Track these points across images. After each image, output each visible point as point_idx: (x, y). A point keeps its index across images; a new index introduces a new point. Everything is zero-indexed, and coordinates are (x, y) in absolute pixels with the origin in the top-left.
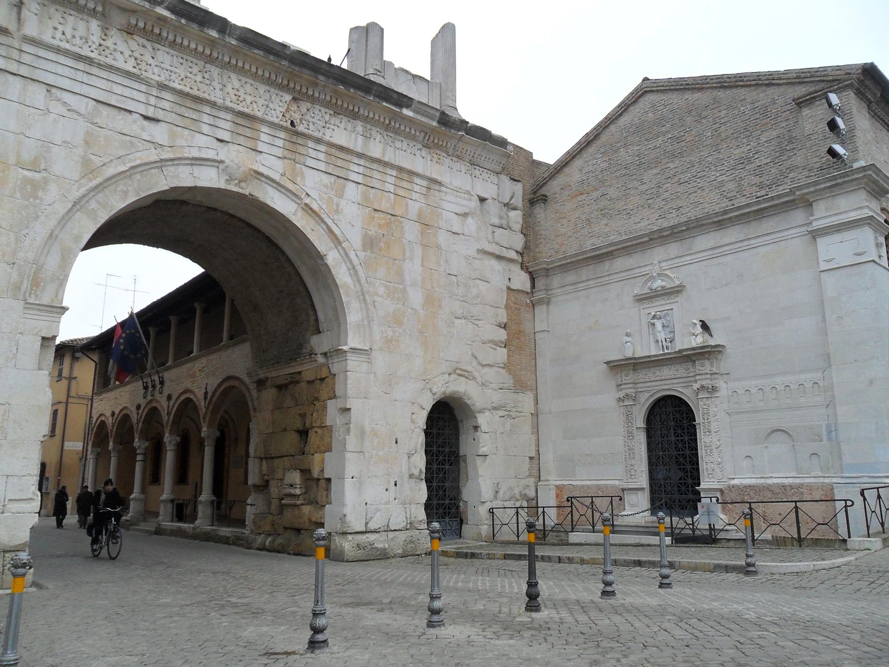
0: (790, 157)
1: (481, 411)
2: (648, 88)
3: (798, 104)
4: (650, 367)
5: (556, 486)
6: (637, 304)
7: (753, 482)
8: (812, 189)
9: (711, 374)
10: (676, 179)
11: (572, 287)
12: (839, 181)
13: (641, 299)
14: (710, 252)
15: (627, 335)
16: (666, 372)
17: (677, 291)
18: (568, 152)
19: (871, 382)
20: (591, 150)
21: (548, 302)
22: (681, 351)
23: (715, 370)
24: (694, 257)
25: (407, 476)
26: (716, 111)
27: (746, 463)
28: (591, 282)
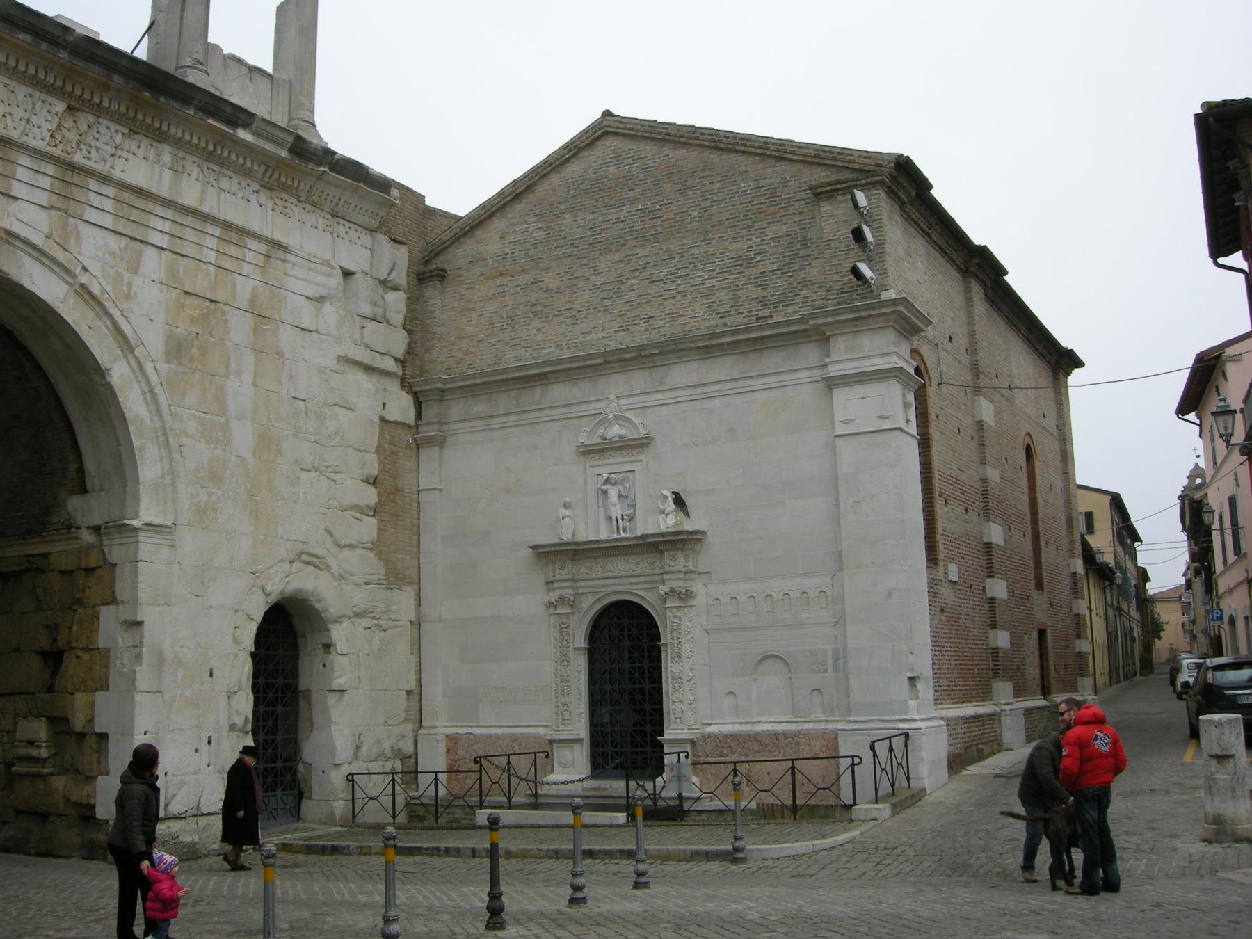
0: (802, 268)
1: (336, 621)
2: (608, 128)
3: (817, 195)
4: (597, 557)
5: (448, 736)
7: (736, 728)
8: (830, 320)
9: (686, 573)
10: (646, 274)
11: (480, 423)
12: (864, 314)
13: (587, 452)
14: (690, 391)
15: (566, 506)
16: (622, 566)
17: (642, 444)
18: (483, 206)
19: (890, 594)
20: (520, 207)
21: (441, 442)
22: (644, 537)
23: (691, 567)
24: (668, 395)
25: (226, 728)
26: (706, 181)
27: (727, 702)
28: (512, 418)
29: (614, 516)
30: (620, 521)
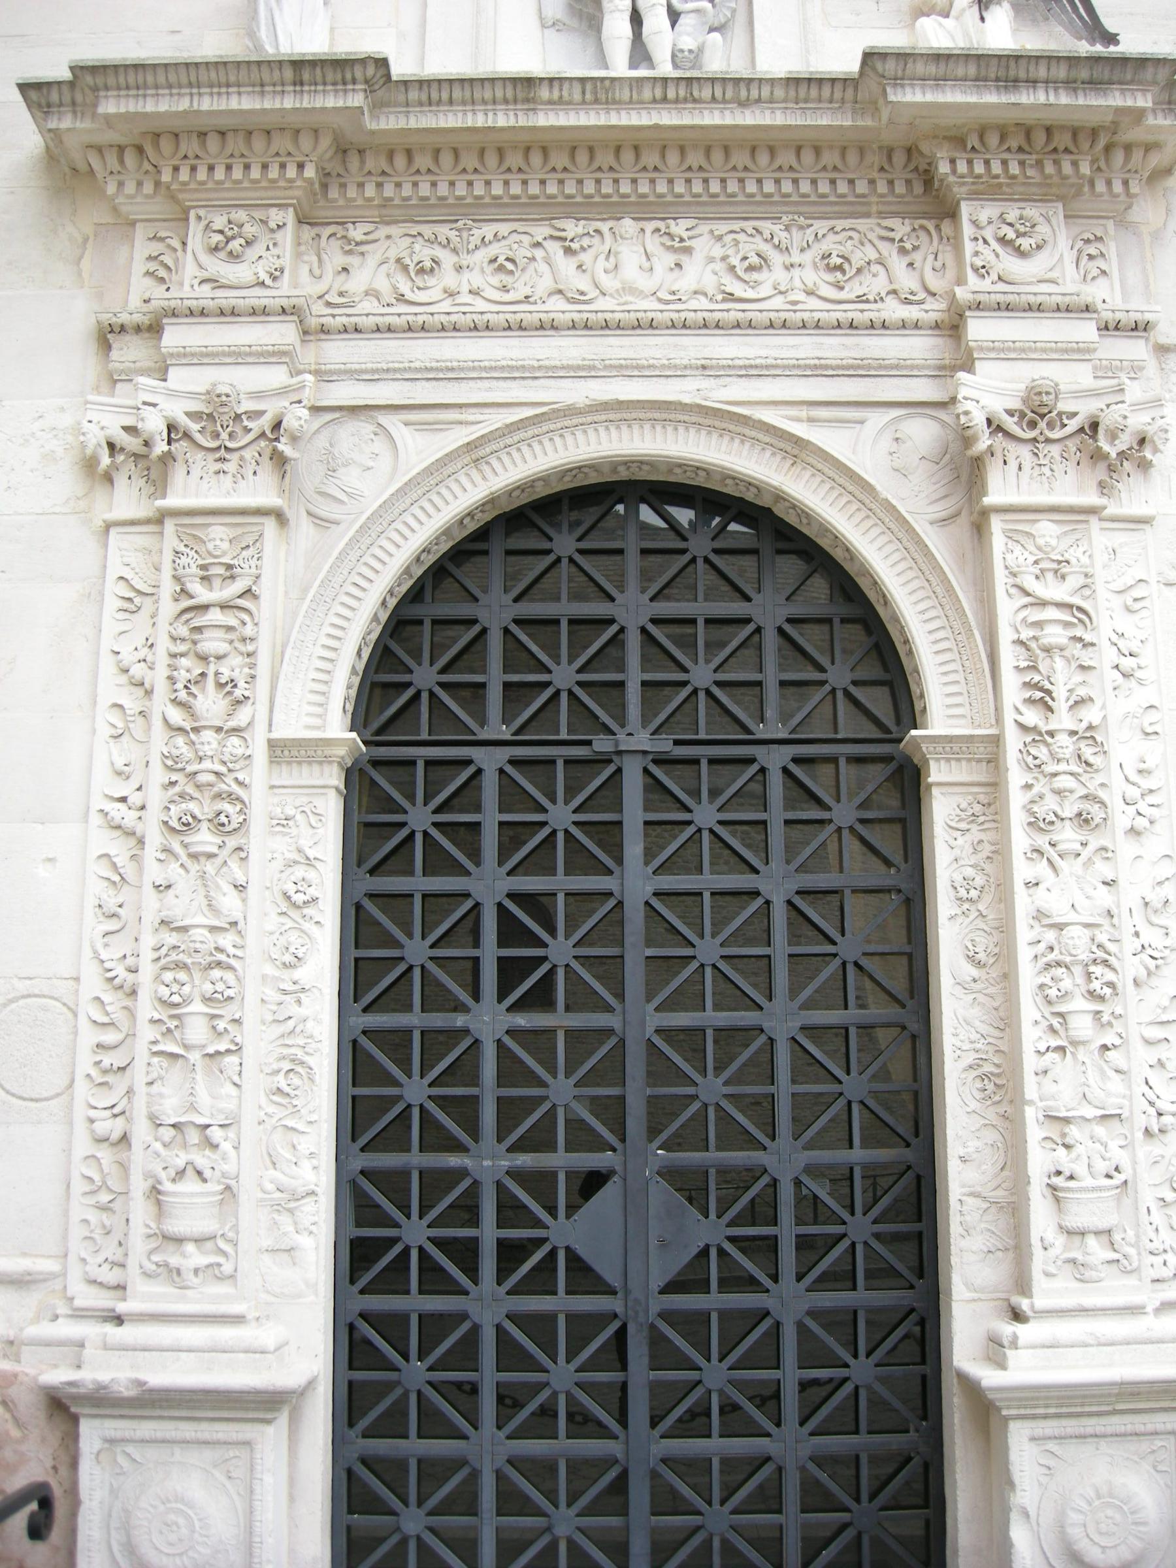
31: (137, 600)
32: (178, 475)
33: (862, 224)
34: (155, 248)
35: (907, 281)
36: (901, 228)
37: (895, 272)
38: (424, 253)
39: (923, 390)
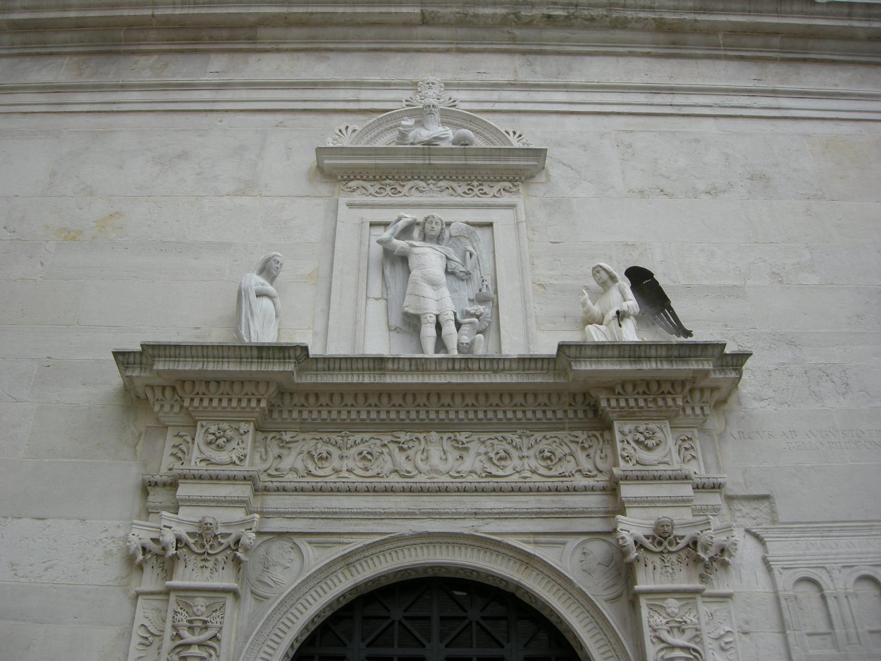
4: (354, 426)
6: (324, 189)
14: (642, 98)
29: (430, 308)
30: (449, 328)
31: (150, 639)
32: (180, 569)
33: (560, 434)
34: (178, 441)
35: (586, 465)
36: (582, 436)
37: (580, 461)
38: (323, 449)
39: (597, 525)
